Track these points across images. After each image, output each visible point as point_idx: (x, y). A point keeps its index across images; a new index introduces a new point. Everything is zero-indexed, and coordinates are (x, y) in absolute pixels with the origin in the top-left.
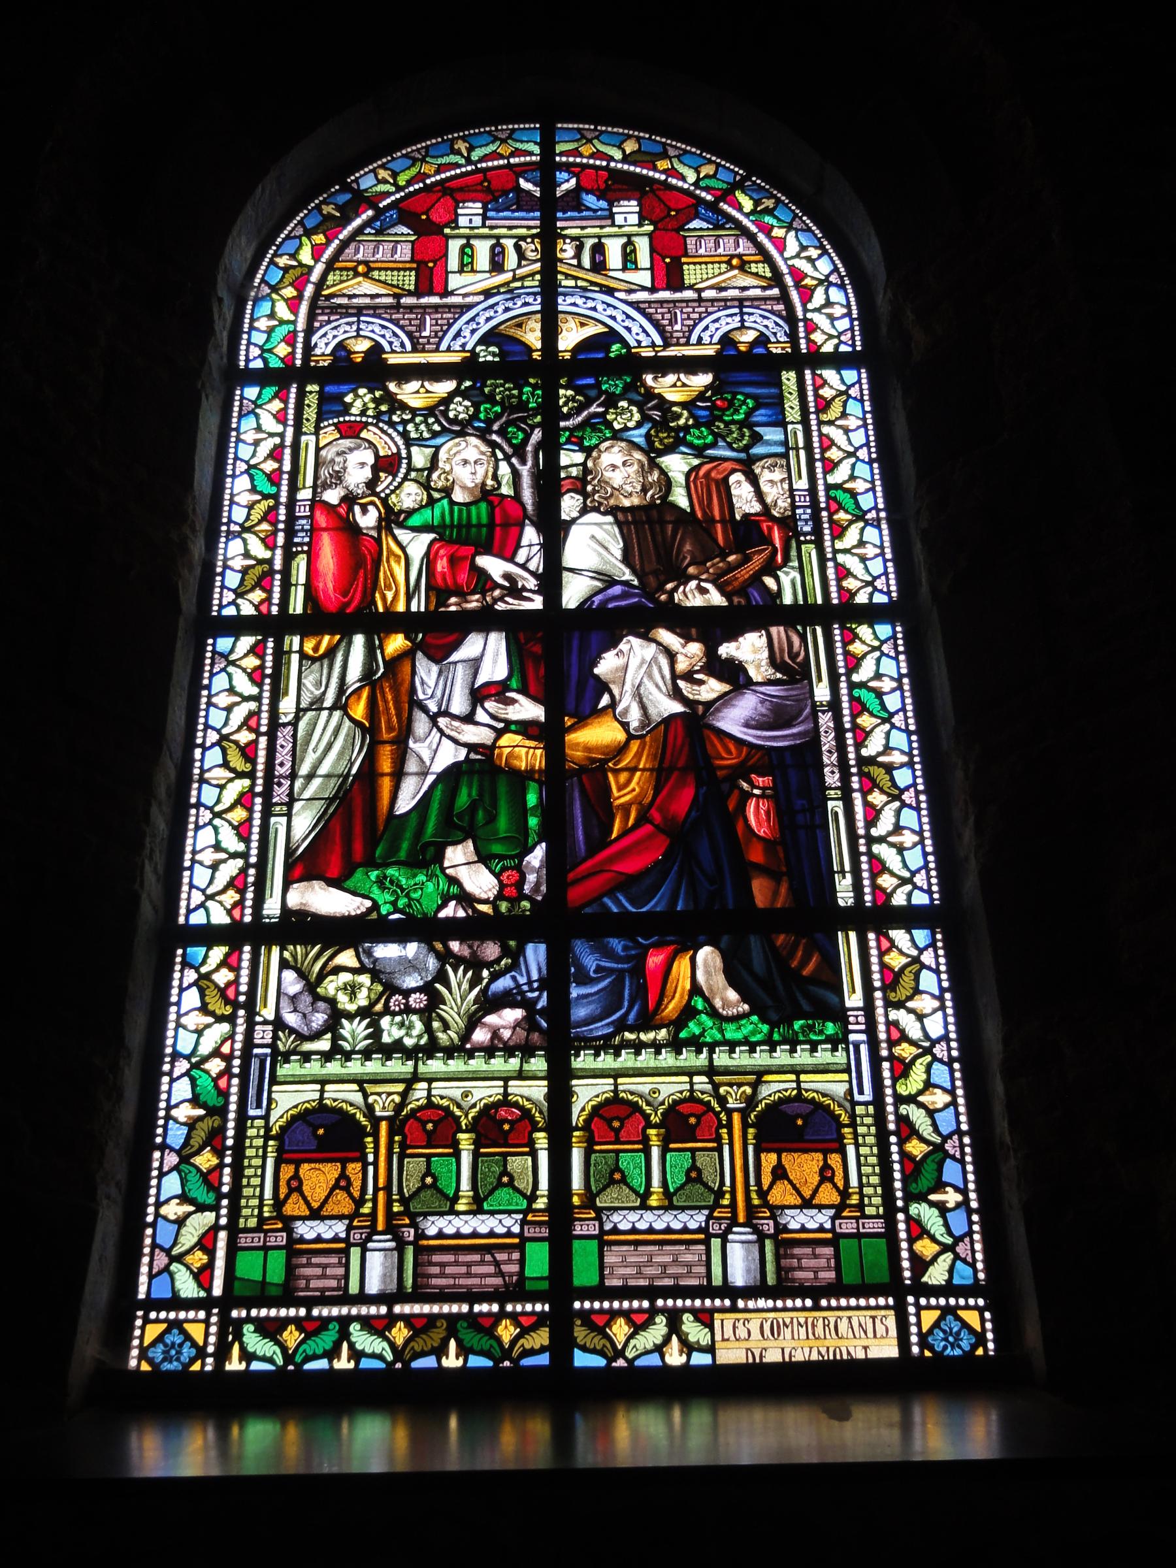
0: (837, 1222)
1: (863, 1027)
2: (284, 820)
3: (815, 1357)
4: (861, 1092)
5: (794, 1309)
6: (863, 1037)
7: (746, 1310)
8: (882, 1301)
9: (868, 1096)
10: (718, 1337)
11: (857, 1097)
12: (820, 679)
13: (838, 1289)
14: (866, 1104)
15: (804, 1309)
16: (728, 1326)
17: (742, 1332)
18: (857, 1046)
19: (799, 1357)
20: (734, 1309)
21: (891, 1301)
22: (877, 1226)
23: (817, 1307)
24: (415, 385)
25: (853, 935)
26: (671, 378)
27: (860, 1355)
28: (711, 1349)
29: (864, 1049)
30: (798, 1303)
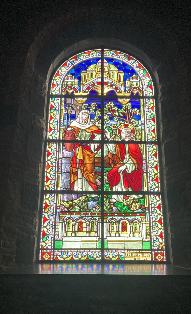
0: (143, 240)
1: (148, 210)
2: (61, 174)
3: (139, 260)
4: (147, 220)
5: (137, 252)
6: (148, 212)
7: (129, 252)
8: (149, 252)
9: (148, 221)
10: (125, 256)
11: (147, 221)
12: (144, 154)
13: (143, 250)
14: (148, 222)
15: (138, 252)
16: (127, 254)
17: (128, 255)
18: (147, 213)
19: (137, 259)
20: (128, 252)
21: (150, 252)
22: (149, 240)
23: (140, 252)
24: (79, 99)
25: (147, 196)
26: (122, 100)
27: (146, 260)
28: (124, 257)
29: (148, 214)
30: (137, 251)
